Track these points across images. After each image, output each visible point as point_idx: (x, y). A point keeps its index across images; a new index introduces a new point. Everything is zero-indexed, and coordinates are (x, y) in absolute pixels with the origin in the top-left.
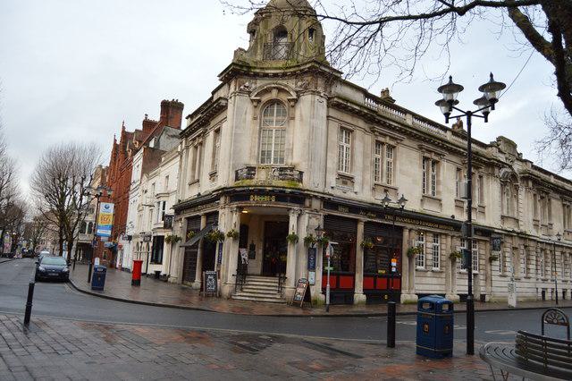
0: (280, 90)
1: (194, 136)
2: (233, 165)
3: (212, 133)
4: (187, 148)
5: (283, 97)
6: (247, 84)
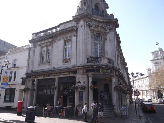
0: (102, 27)
1: (43, 42)
2: (86, 56)
3: (61, 42)
4: (35, 47)
6: (89, 22)
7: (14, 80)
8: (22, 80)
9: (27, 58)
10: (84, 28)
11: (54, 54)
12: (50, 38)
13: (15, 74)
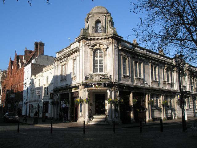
1: (61, 61)
3: (72, 61)
4: (58, 65)
7: (47, 95)
12: (65, 57)
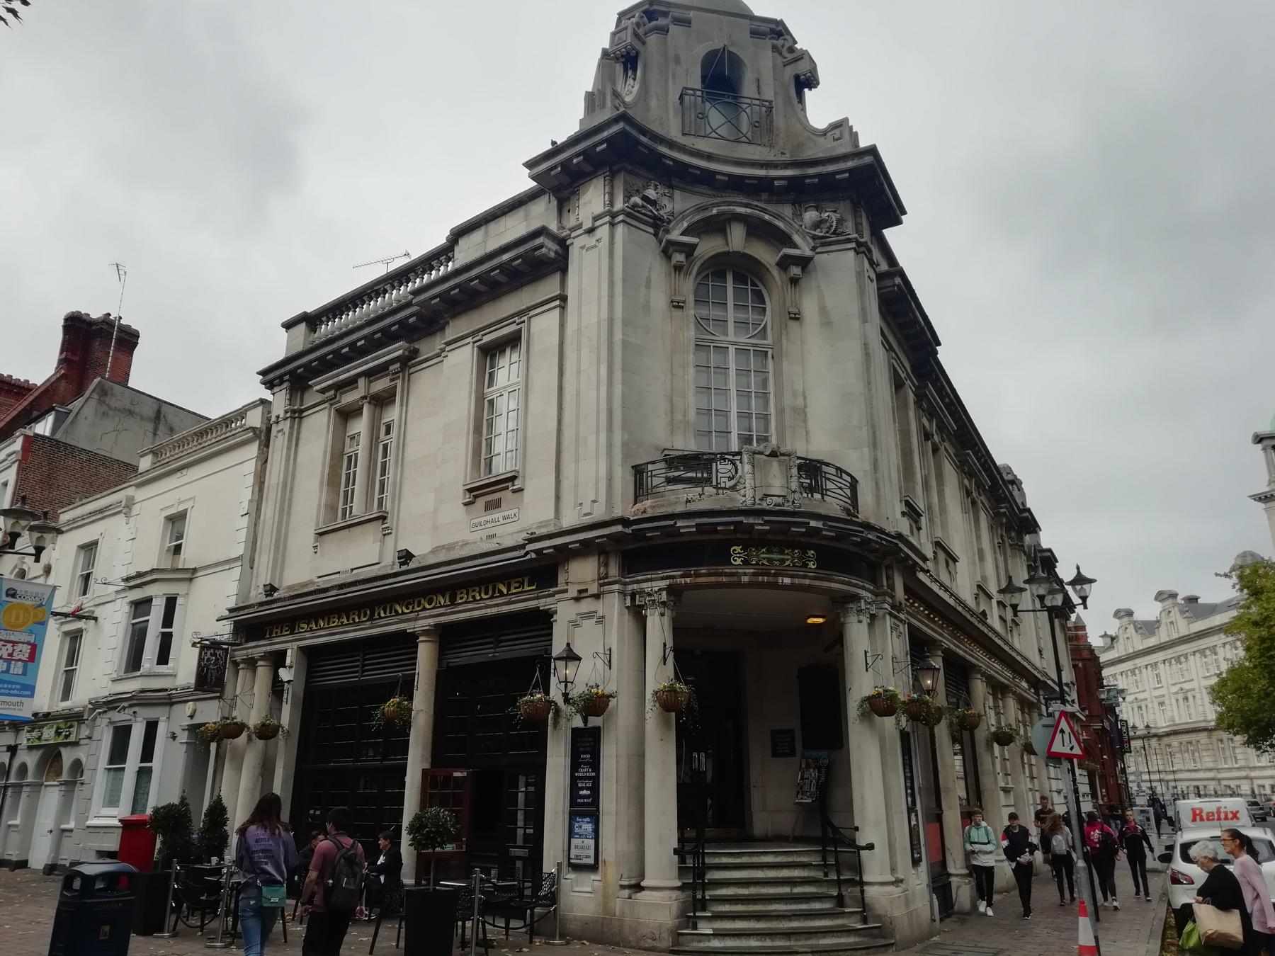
1: (343, 374)
2: (625, 445)
3: (463, 359)
4: (297, 415)
5: (766, 255)
6: (651, 193)
7: (163, 658)
8: (201, 659)
9: (247, 494)
10: (612, 236)
11: (412, 453)
12: (388, 337)
13: (168, 620)
